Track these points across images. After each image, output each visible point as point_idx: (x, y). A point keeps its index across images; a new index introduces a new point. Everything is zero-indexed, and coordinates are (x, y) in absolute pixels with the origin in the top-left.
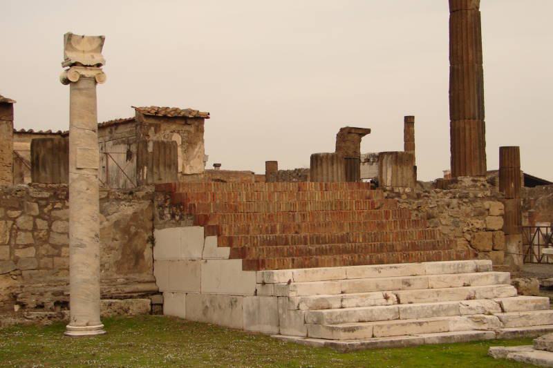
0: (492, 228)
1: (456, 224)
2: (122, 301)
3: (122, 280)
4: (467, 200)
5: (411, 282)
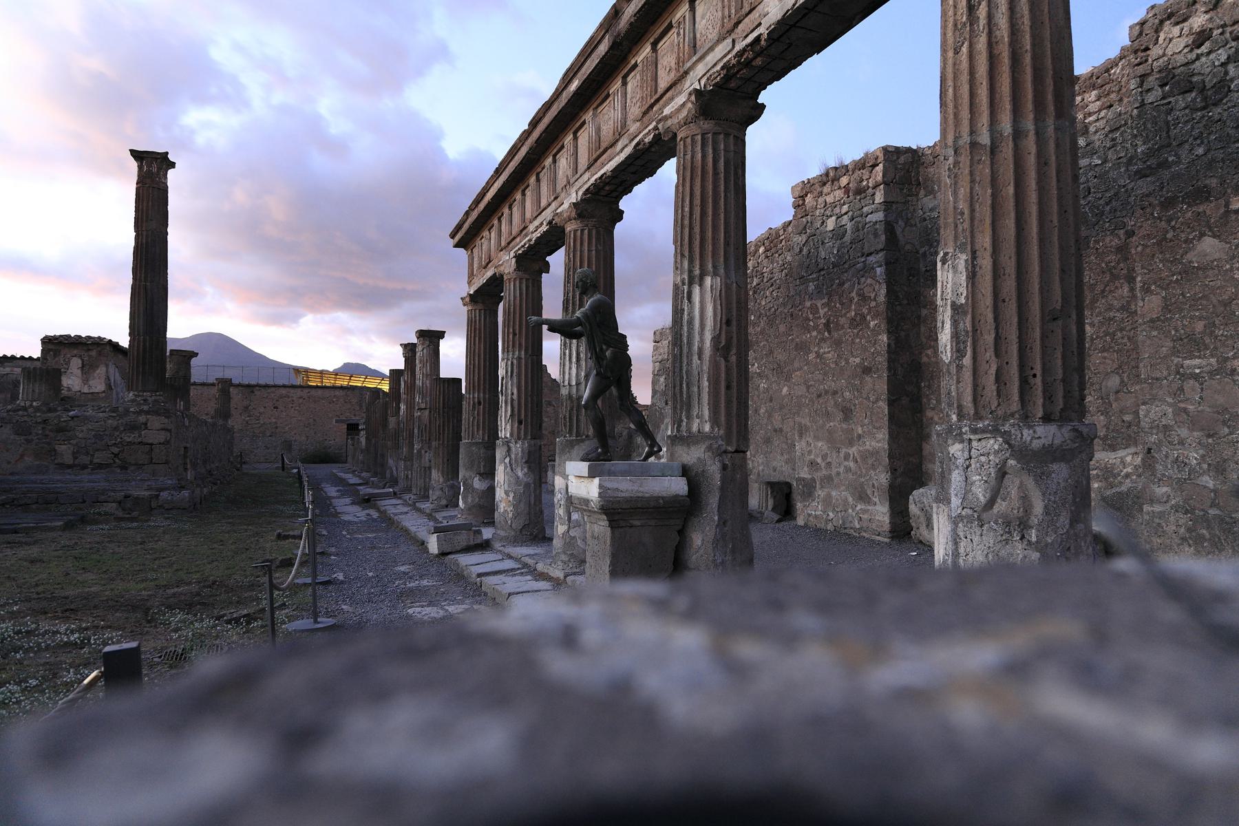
0: (150, 441)
4: (114, 414)
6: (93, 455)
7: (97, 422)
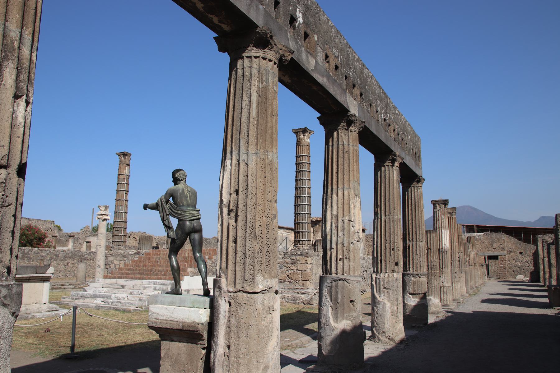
4: (287, 256)
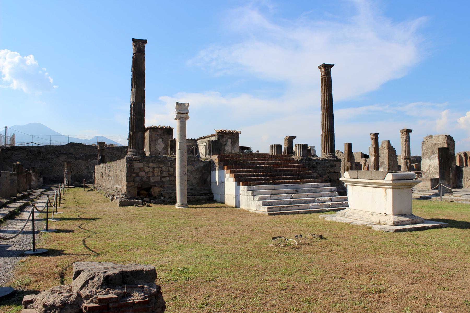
0: (337, 171)
1: (323, 170)
2: (199, 196)
3: (199, 189)
4: (327, 161)
5: (298, 191)
6: (322, 177)
7: (322, 164)
